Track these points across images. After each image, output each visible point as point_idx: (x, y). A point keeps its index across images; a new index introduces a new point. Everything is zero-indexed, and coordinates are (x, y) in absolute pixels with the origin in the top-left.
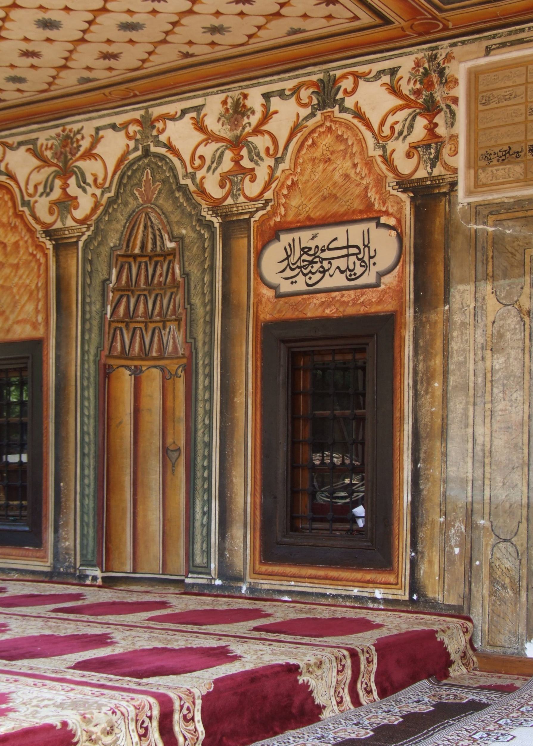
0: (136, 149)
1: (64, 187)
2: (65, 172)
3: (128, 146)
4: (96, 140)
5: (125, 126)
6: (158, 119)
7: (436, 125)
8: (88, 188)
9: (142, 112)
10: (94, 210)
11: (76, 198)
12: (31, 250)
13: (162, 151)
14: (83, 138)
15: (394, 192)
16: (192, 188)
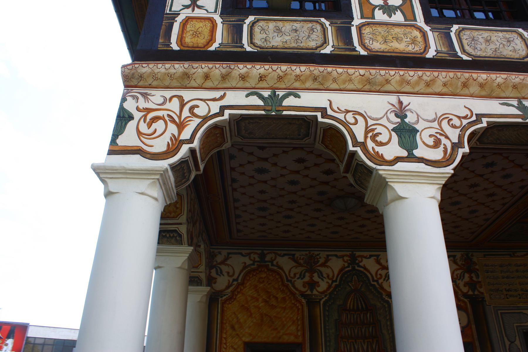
0: (348, 267)
1: (311, 277)
2: (312, 271)
3: (344, 265)
4: (327, 260)
5: (342, 257)
6: (359, 256)
7: (472, 277)
8: (324, 279)
9: (350, 253)
10: (328, 289)
11: (318, 282)
12: (293, 302)
13: (362, 269)
14: (320, 258)
15: (462, 298)
16: (377, 286)
